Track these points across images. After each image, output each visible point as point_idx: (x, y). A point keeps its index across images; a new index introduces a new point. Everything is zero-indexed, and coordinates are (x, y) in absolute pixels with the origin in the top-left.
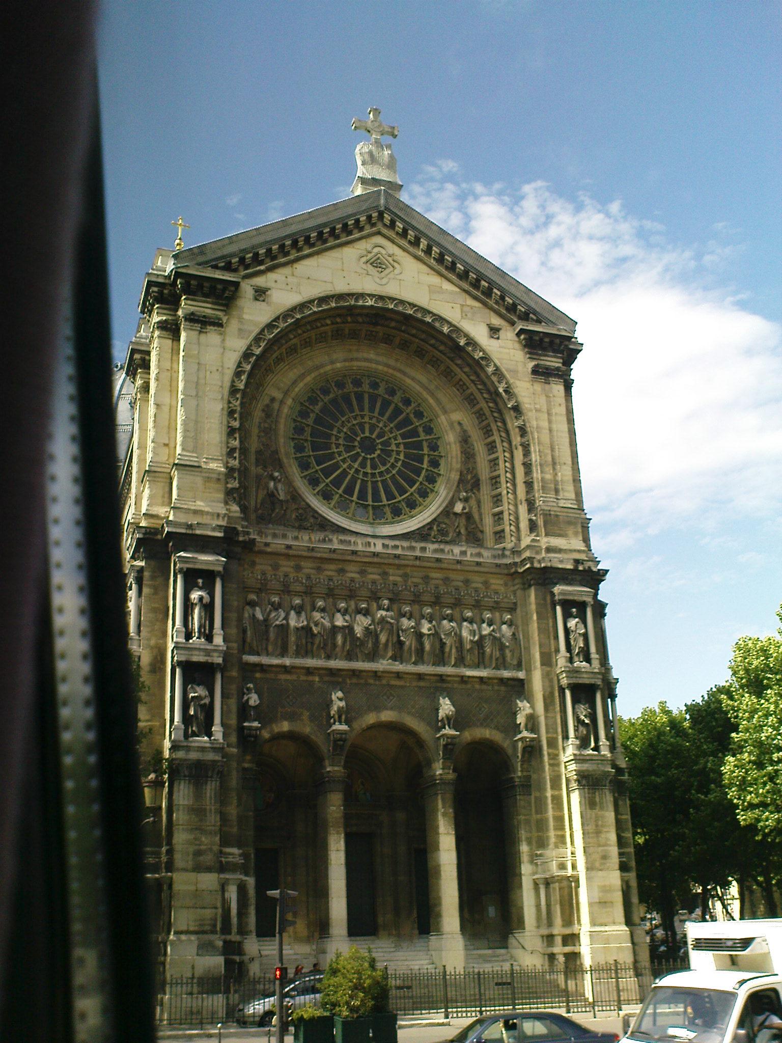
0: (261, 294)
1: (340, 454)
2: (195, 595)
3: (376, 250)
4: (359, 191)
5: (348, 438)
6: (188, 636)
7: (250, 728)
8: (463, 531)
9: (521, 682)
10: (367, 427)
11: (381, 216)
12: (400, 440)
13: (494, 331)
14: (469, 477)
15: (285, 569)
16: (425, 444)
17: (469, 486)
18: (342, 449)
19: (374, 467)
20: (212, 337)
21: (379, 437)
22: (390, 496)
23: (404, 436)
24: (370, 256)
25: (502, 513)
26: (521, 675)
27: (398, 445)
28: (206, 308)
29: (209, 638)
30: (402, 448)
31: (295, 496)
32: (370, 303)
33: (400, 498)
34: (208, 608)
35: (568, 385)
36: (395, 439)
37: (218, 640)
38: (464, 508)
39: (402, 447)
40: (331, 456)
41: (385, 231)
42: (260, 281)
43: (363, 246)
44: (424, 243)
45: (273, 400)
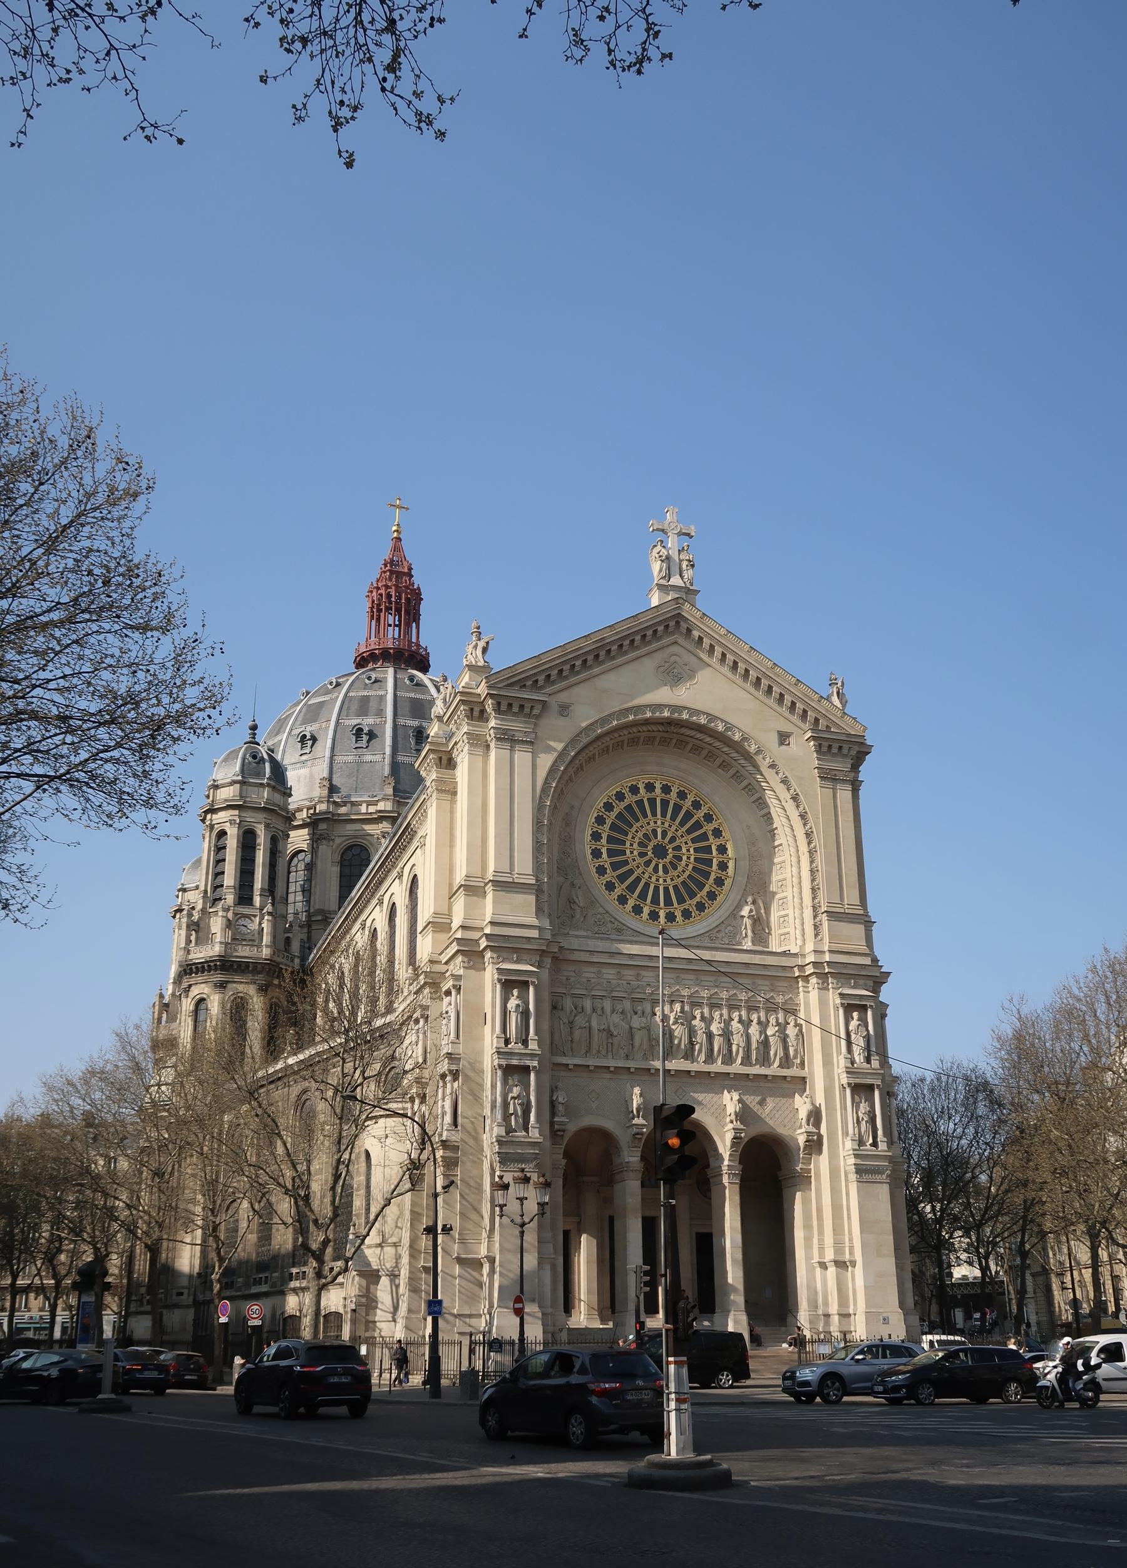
0: (564, 710)
2: (513, 1003)
3: (673, 658)
4: (655, 601)
5: (641, 844)
6: (507, 1042)
7: (560, 1123)
9: (803, 1080)
10: (659, 831)
11: (678, 623)
13: (783, 738)
15: (587, 975)
16: (714, 848)
19: (666, 871)
21: (671, 842)
24: (667, 665)
25: (787, 916)
26: (802, 1074)
28: (516, 726)
29: (525, 1043)
30: (692, 851)
31: (593, 902)
32: (666, 714)
34: (525, 1014)
35: (856, 786)
36: (686, 843)
37: (533, 1046)
38: (751, 911)
41: (681, 641)
42: (563, 697)
43: (659, 657)
44: (718, 650)
45: (572, 807)
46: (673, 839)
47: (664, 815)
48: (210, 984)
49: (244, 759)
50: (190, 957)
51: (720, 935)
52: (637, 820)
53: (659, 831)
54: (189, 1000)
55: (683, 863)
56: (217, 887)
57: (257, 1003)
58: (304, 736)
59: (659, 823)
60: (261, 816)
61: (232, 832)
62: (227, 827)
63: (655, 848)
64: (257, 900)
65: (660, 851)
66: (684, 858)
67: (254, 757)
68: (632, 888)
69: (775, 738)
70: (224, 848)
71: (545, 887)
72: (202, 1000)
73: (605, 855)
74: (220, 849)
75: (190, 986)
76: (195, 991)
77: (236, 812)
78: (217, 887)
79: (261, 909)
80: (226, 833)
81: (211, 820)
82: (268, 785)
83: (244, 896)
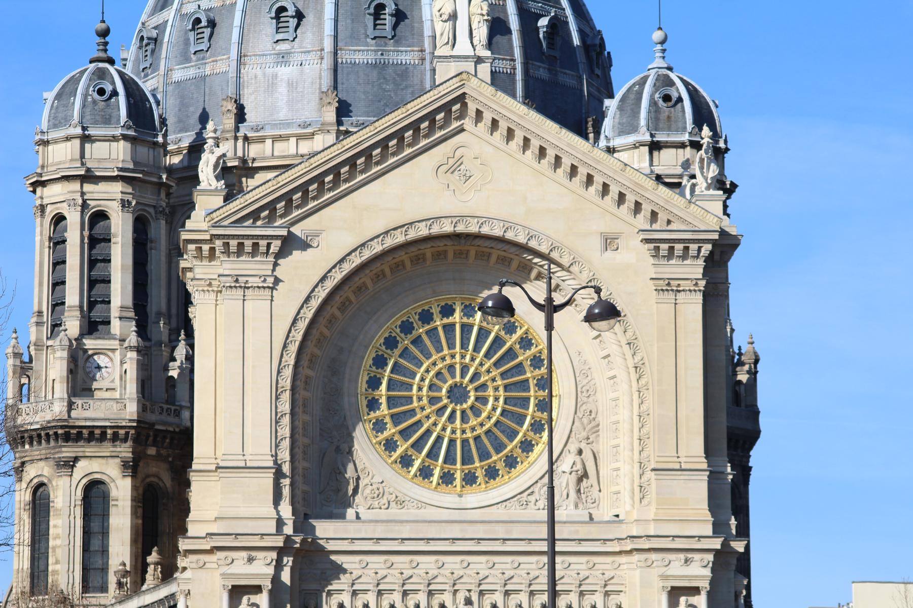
1: (423, 409)
3: (458, 154)
8: (573, 494)
10: (458, 367)
11: (465, 105)
12: (499, 382)
13: (609, 242)
14: (585, 420)
16: (532, 383)
17: (584, 434)
18: (425, 401)
19: (464, 419)
20: (257, 305)
22: (484, 455)
23: (503, 375)
24: (451, 162)
25: (618, 469)
27: (496, 389)
33: (495, 458)
39: (501, 389)
40: (412, 412)
46: (476, 376)
47: (464, 346)
48: (52, 463)
49: (85, 96)
50: (19, 421)
51: (532, 499)
52: (428, 356)
53: (458, 367)
54: (24, 485)
55: (489, 406)
56: (58, 304)
57: (122, 491)
58: (198, 21)
59: (458, 357)
60: (116, 189)
61: (73, 218)
62: (64, 209)
63: (450, 391)
64: (116, 326)
65: (457, 394)
66: (491, 400)
67: (101, 92)
68: (418, 445)
69: (597, 243)
70: (64, 241)
71: (286, 468)
72: (41, 485)
73: (384, 406)
74: (58, 242)
75: (23, 464)
76: (31, 472)
77: (76, 186)
78: (58, 304)
79: (122, 340)
80: (64, 218)
81: (42, 198)
82: (125, 137)
83: (94, 325)
